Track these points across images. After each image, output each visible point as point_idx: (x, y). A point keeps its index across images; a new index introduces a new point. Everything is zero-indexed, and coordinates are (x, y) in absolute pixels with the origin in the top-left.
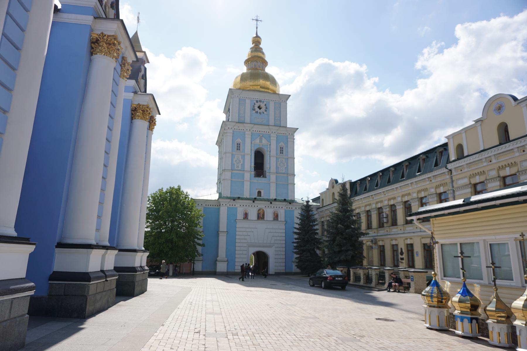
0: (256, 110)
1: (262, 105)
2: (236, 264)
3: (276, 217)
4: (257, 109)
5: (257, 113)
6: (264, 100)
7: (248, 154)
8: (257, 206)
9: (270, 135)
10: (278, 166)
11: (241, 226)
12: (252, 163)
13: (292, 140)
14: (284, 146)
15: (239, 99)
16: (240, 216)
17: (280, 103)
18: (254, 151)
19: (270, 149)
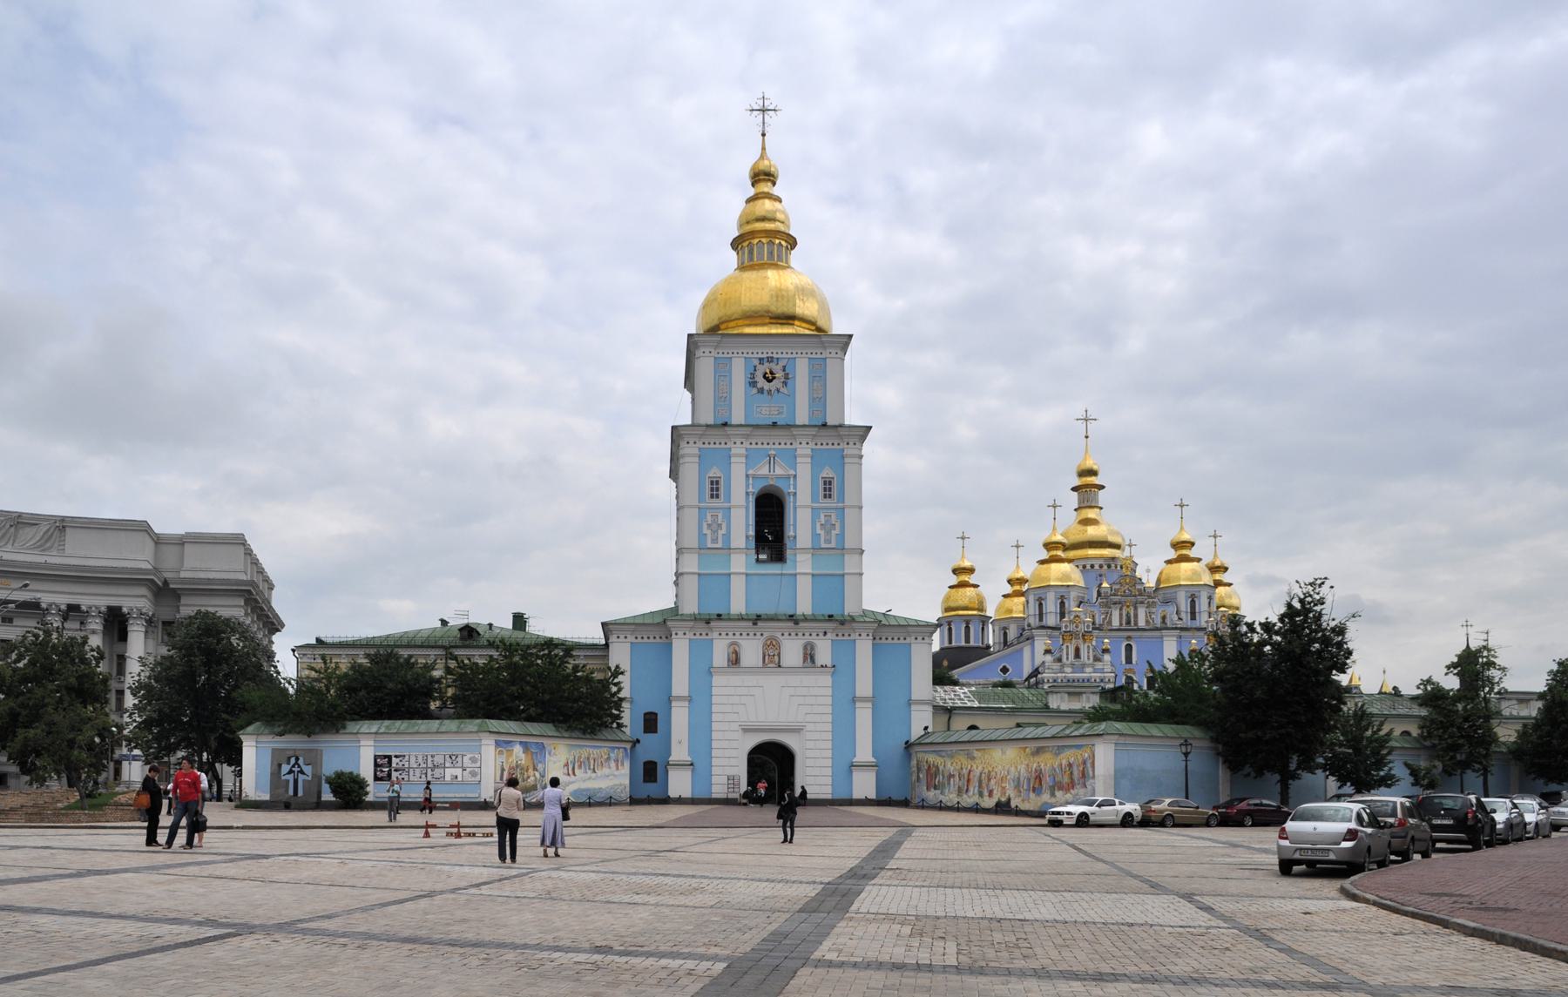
0: (759, 386)
1: (777, 369)
2: (715, 770)
3: (809, 656)
4: (762, 383)
5: (762, 393)
6: (780, 356)
7: (739, 507)
8: (762, 635)
9: (796, 450)
10: (819, 531)
11: (722, 684)
12: (751, 527)
13: (856, 460)
14: (833, 478)
15: (715, 358)
16: (720, 656)
17: (826, 358)
18: (755, 497)
19: (795, 488)
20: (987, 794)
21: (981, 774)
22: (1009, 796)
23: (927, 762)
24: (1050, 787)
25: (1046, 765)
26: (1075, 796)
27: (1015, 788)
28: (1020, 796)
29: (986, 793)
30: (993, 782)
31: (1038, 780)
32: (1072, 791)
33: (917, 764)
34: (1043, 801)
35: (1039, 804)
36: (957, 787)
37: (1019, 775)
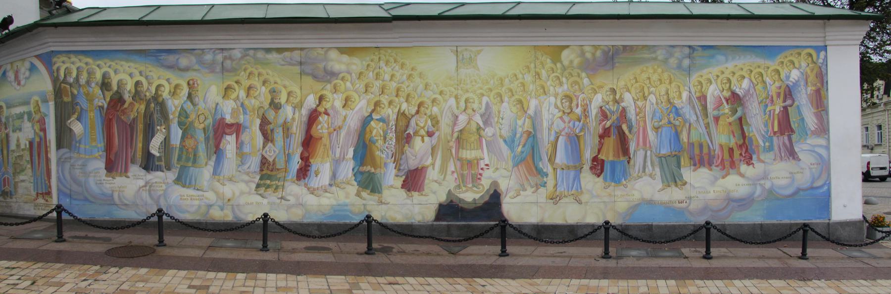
20: (399, 182)
21: (366, 122)
22: (495, 184)
23: (105, 85)
24: (661, 157)
25: (645, 98)
26: (754, 182)
27: (518, 162)
28: (544, 185)
29: (391, 178)
30: (420, 146)
31: (611, 142)
32: (744, 168)
33: (58, 93)
34: (636, 196)
35: (622, 206)
36: (254, 163)
37: (535, 120)
